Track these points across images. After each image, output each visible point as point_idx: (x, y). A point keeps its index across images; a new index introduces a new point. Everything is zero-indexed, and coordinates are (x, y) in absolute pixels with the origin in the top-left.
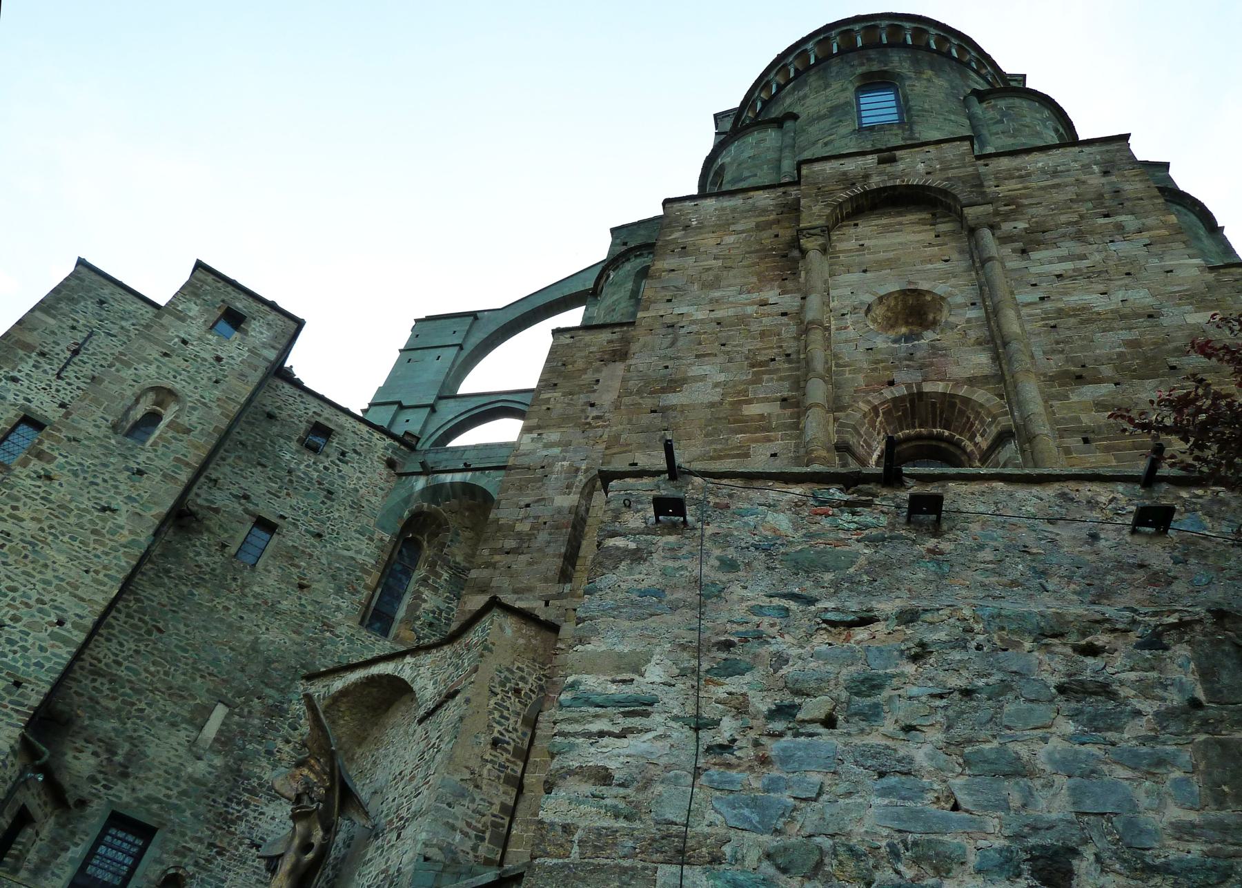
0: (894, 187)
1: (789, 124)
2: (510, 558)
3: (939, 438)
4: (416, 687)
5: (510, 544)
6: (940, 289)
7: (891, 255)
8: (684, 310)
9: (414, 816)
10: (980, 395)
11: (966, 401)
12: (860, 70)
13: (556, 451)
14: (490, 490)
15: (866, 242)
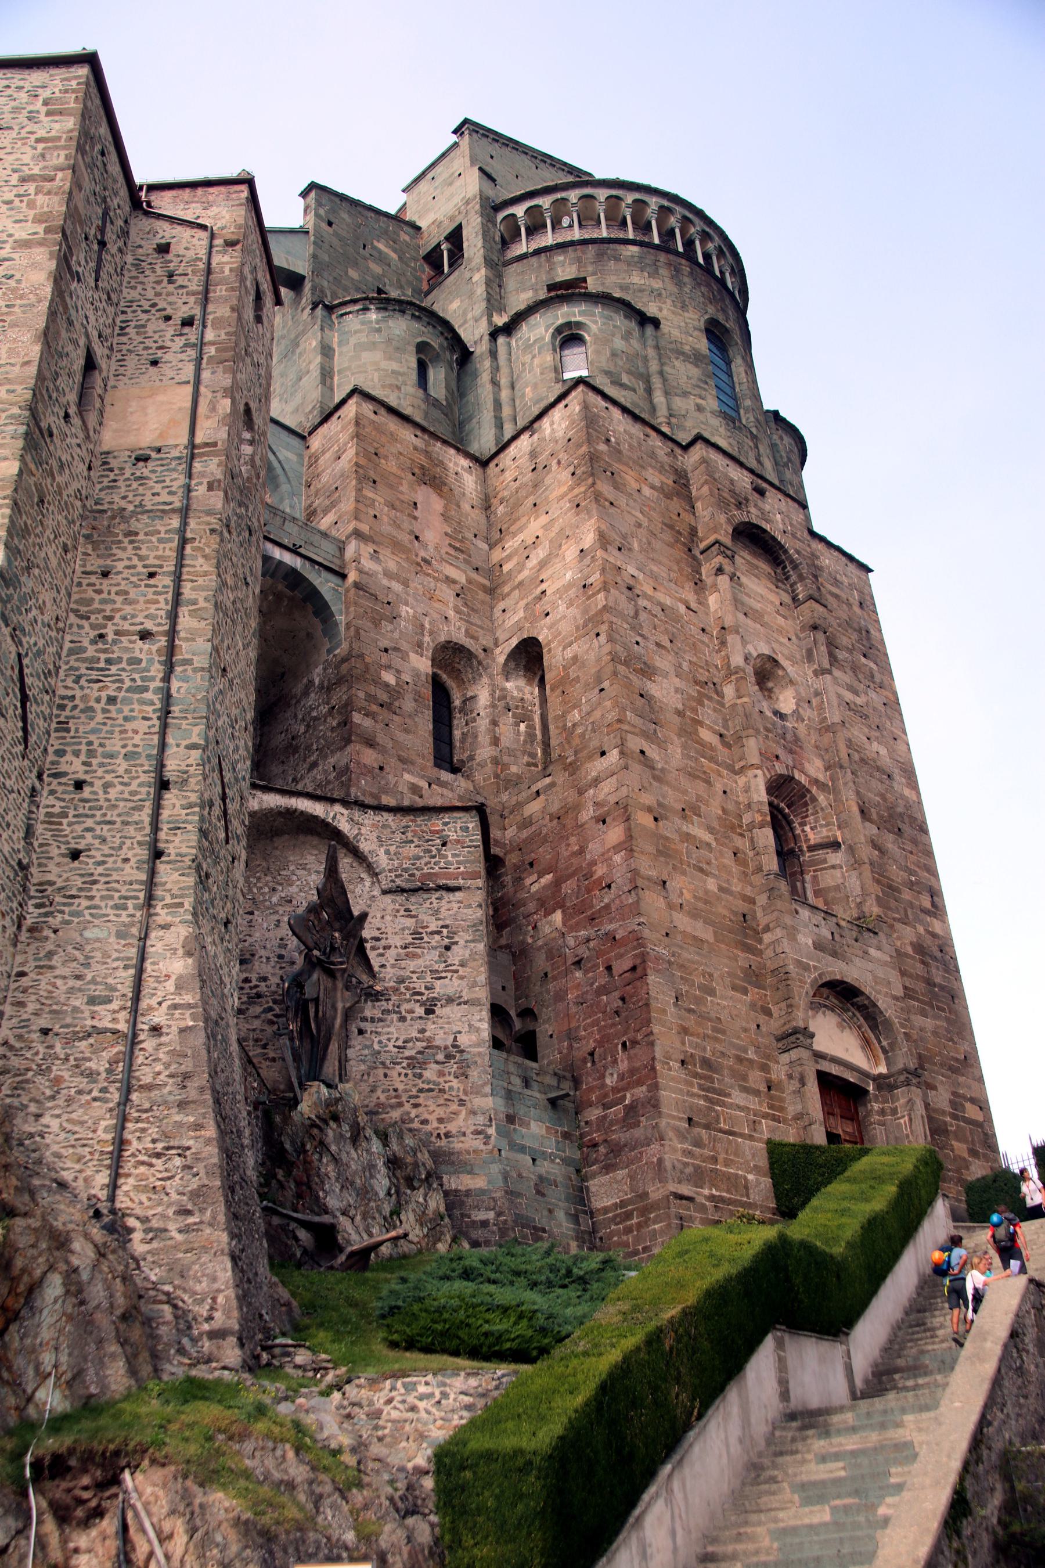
0: (765, 531)
1: (649, 330)
2: (384, 714)
3: (781, 811)
4: (364, 847)
5: (384, 697)
6: (790, 669)
7: (758, 606)
8: (636, 573)
9: (450, 1000)
10: (821, 798)
11: (814, 799)
12: (711, 310)
13: (397, 587)
14: (327, 596)
15: (744, 580)
